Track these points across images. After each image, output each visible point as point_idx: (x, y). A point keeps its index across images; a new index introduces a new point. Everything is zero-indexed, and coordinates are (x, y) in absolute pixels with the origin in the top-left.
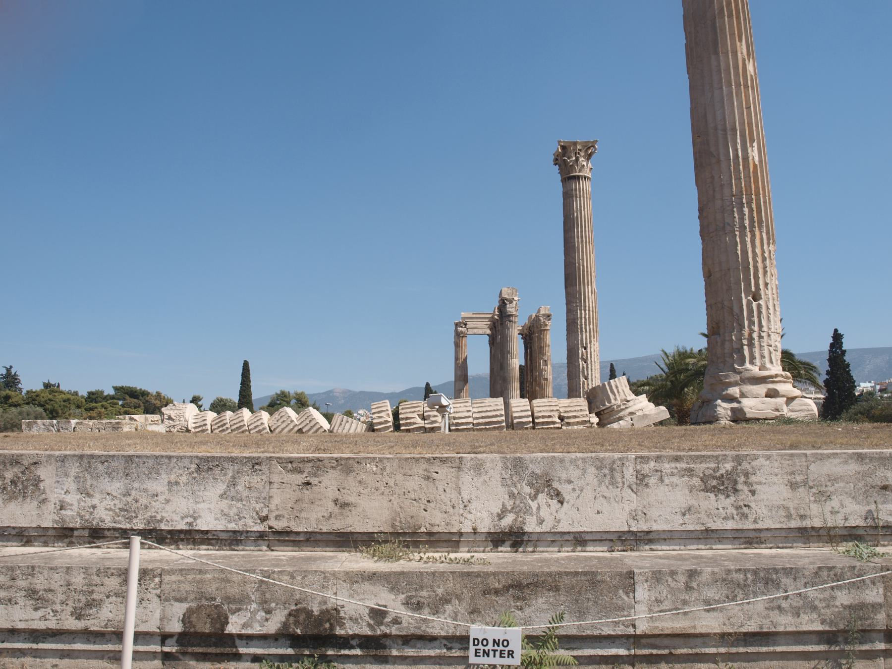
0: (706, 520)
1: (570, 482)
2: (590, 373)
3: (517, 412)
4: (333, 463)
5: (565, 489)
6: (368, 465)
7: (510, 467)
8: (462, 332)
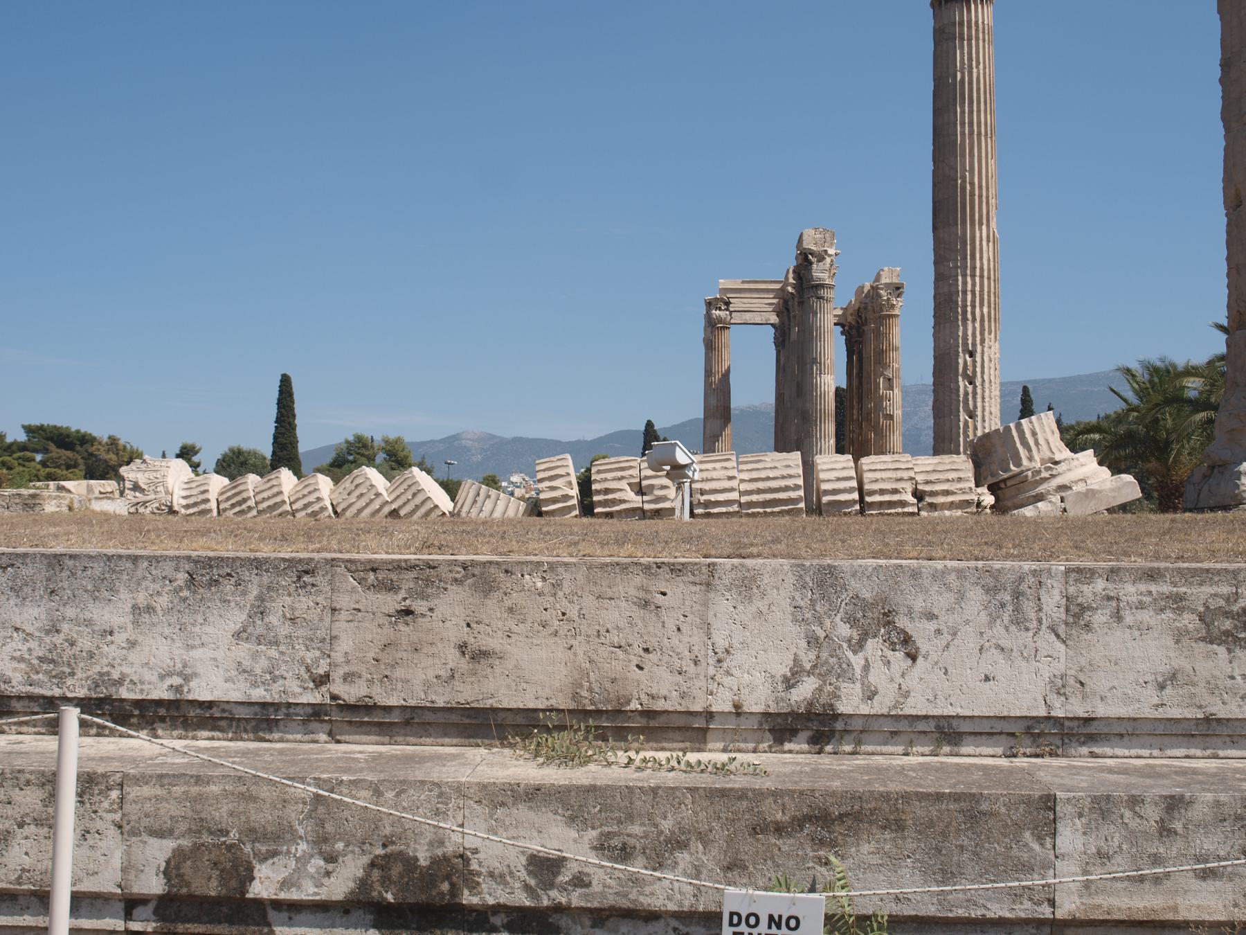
0: (1206, 699)
1: (931, 616)
2: (979, 404)
3: (828, 481)
4: (458, 572)
5: (921, 631)
6: (527, 577)
7: (811, 585)
8: (720, 320)
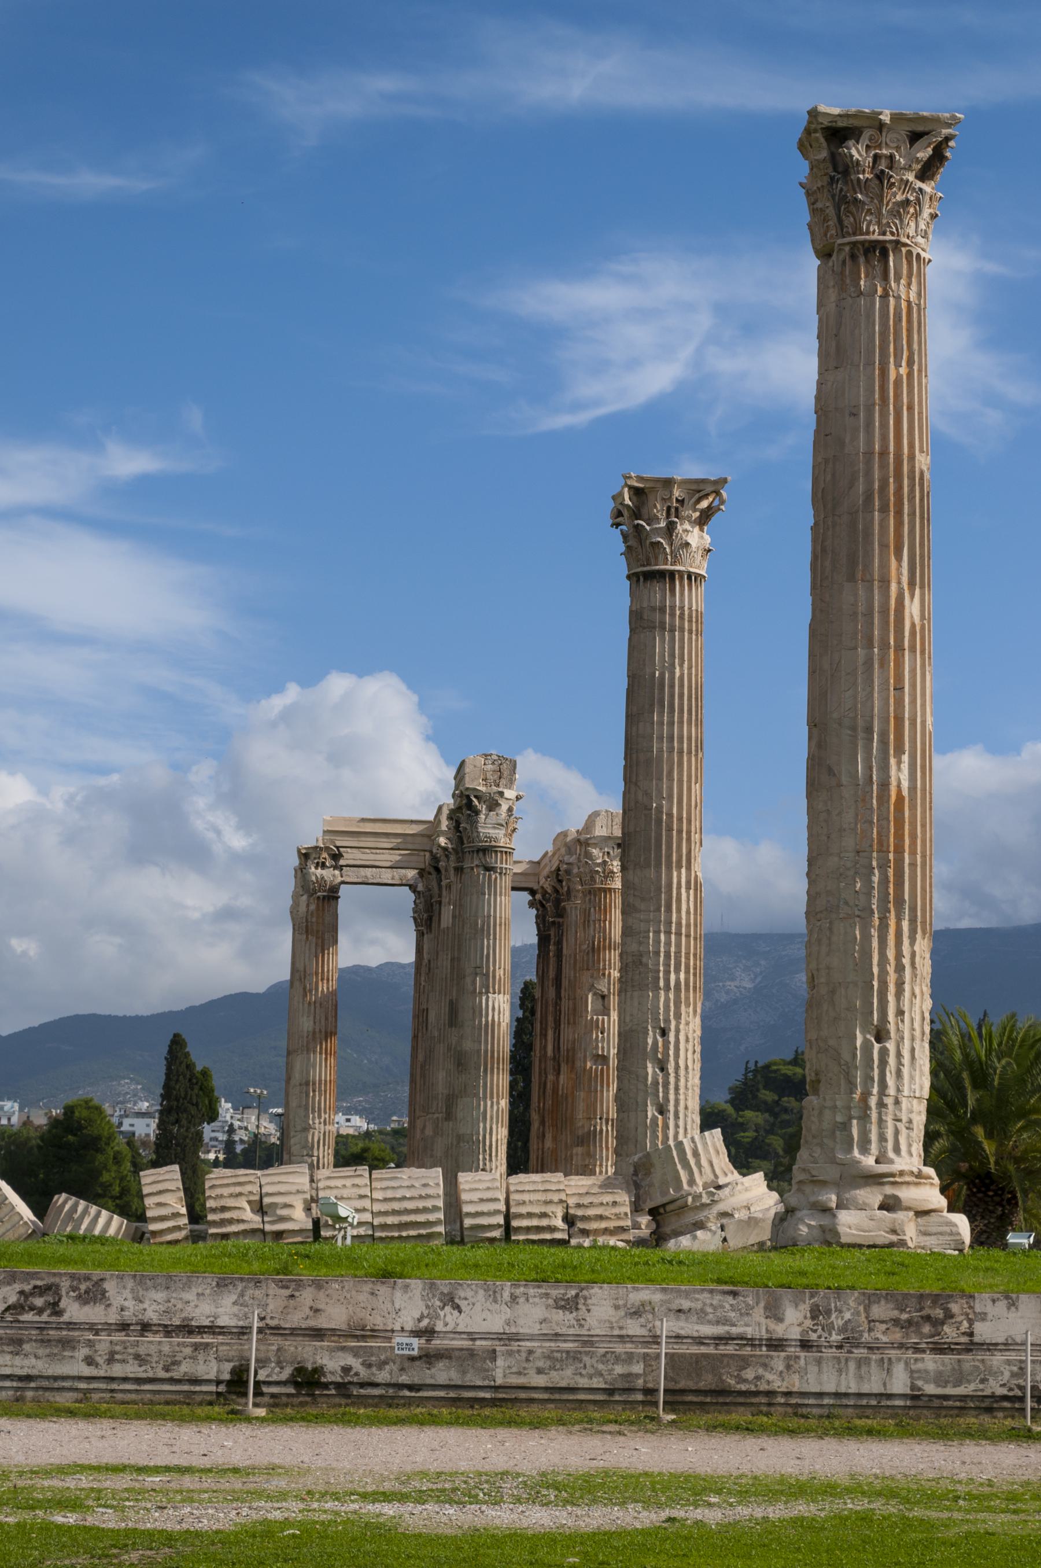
0: (556, 1327)
1: (466, 1299)
2: (672, 1097)
5: (463, 1304)
